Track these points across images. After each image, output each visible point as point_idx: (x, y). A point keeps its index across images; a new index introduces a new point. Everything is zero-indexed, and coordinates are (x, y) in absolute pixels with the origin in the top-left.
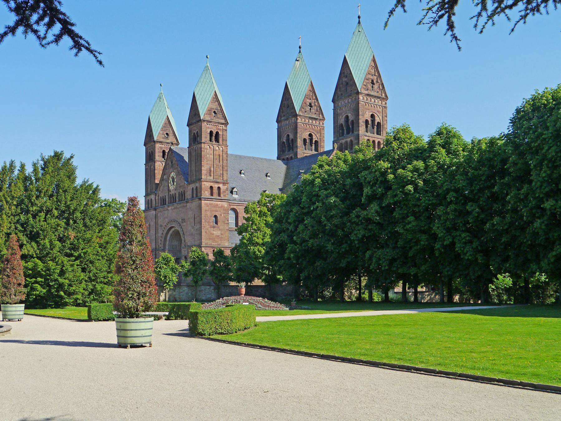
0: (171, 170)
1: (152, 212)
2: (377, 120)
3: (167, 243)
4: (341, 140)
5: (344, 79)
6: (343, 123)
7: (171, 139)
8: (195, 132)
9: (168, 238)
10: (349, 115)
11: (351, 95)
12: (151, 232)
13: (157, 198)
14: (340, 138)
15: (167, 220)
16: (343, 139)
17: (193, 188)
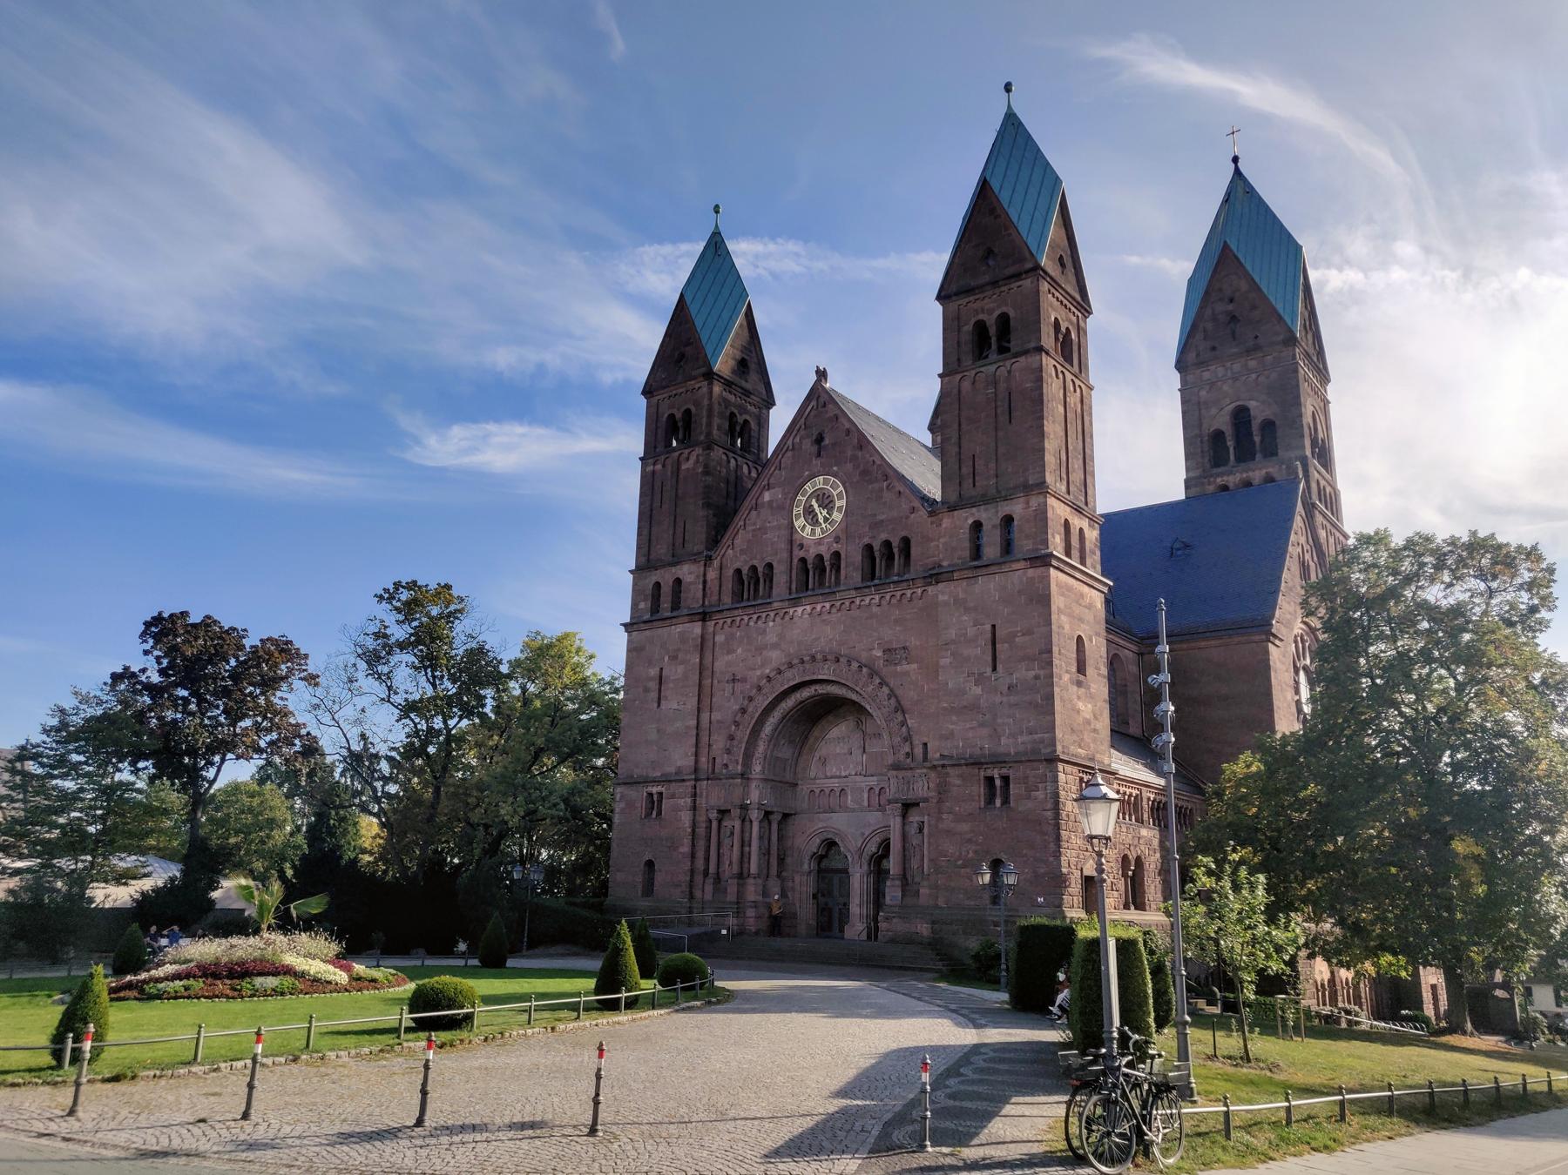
0: (816, 462)
1: (680, 628)
2: (1321, 435)
3: (761, 747)
4: (1218, 475)
5: (1221, 307)
6: (1228, 431)
7: (752, 382)
8: (991, 320)
9: (768, 729)
10: (1252, 404)
11: (1257, 348)
12: (670, 704)
13: (712, 574)
14: (1215, 471)
15: (776, 657)
16: (1230, 473)
17: (977, 525)
